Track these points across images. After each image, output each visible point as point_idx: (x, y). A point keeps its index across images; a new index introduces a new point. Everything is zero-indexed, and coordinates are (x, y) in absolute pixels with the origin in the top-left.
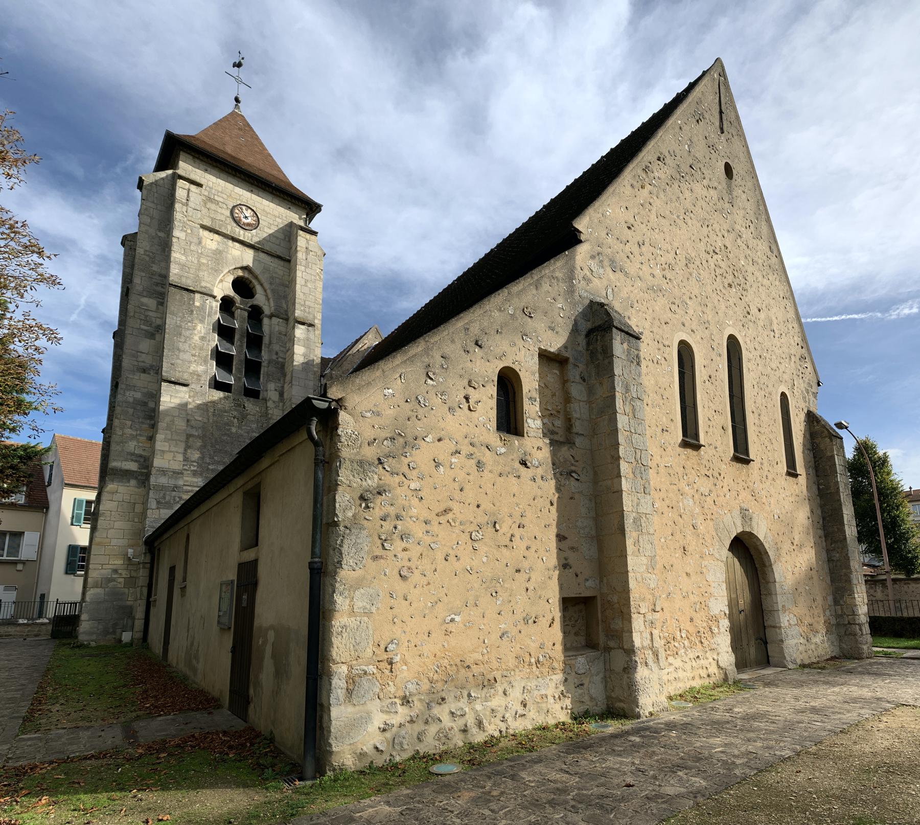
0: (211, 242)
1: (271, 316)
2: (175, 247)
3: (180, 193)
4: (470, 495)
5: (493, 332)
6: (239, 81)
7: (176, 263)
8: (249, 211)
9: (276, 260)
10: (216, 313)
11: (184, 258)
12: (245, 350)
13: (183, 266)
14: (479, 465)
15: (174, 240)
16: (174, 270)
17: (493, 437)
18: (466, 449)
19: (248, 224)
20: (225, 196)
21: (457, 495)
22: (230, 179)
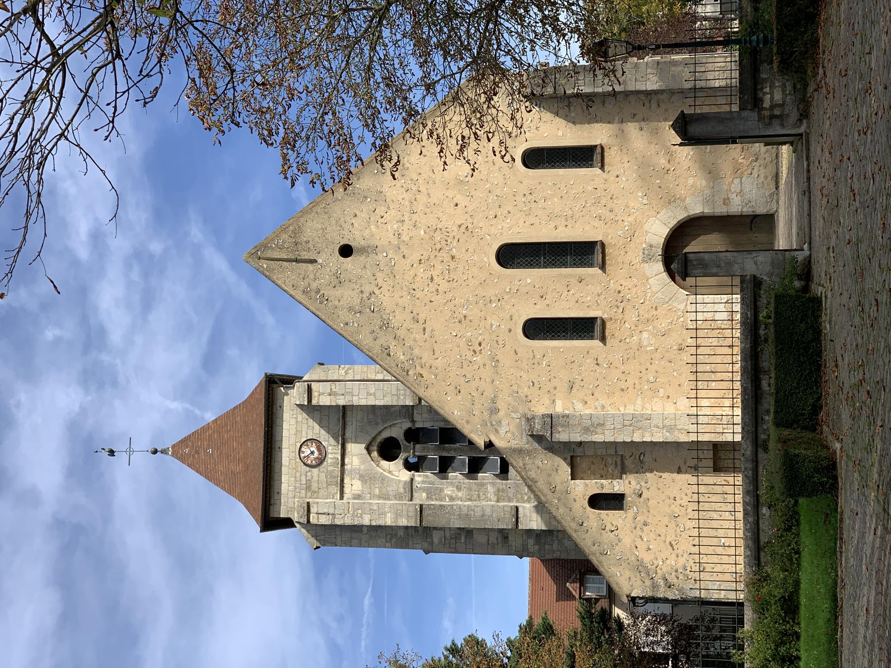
0: (353, 486)
1: (413, 421)
2: (381, 522)
3: (324, 520)
4: (662, 530)
5: (571, 513)
6: (130, 451)
7: (396, 521)
8: (303, 449)
9: (347, 419)
10: (427, 476)
11: (389, 515)
12: (458, 445)
13: (397, 515)
14: (645, 524)
15: (374, 523)
16: (403, 522)
17: (630, 513)
18: (639, 532)
19: (319, 450)
20: (298, 475)
21: (663, 538)
22: (276, 470)
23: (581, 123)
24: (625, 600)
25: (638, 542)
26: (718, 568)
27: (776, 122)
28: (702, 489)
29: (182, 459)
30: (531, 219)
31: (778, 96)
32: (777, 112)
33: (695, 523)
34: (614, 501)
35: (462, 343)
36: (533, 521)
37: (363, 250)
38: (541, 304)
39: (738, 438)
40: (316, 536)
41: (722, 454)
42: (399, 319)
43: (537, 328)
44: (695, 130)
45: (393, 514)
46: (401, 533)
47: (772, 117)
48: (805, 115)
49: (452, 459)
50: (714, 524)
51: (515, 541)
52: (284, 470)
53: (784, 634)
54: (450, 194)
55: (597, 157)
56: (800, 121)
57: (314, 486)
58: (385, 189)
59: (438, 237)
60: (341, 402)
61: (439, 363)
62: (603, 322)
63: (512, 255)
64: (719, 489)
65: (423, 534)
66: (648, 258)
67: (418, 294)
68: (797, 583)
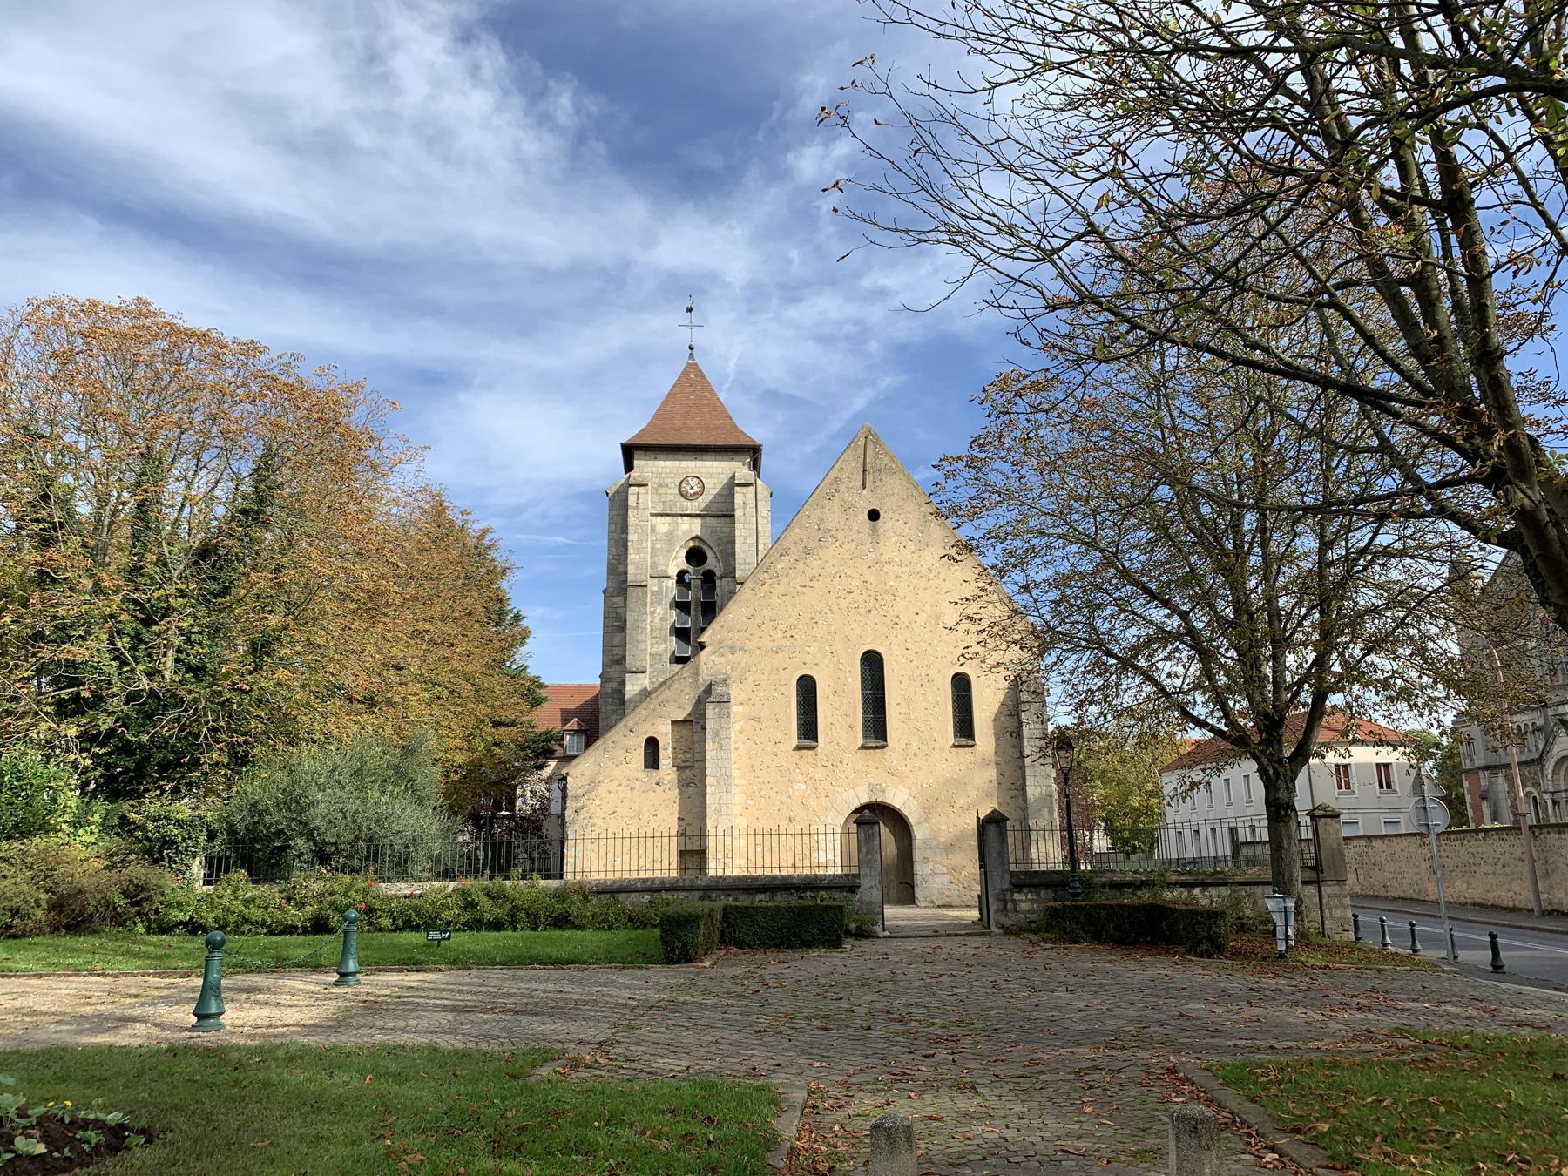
0: (663, 525)
2: (630, 551)
3: (632, 499)
6: (691, 326)
13: (638, 565)
16: (631, 570)
23: (995, 727)
24: (564, 771)
25: (616, 783)
26: (595, 856)
27: (1001, 904)
28: (666, 840)
29: (685, 372)
30: (906, 682)
31: (1024, 907)
32: (1009, 906)
33: (634, 834)
34: (652, 761)
35: (792, 621)
36: (633, 687)
37: (875, 531)
38: (829, 691)
39: (711, 873)
40: (617, 492)
41: (696, 858)
42: (814, 563)
43: (807, 688)
44: (992, 830)
45: (638, 562)
46: (621, 568)
47: (1005, 902)
48: (1008, 931)
49: (688, 613)
50: (634, 851)
51: (614, 671)
52: (676, 463)
53: (537, 916)
54: (927, 608)
55: (964, 741)
56: (1002, 927)
57: (662, 490)
58: (931, 550)
59: (889, 598)
60: (738, 513)
61: (774, 600)
62: (814, 748)
63: (873, 664)
64: (666, 854)
65: (619, 587)
66: (872, 789)
67: (836, 580)
68: (582, 928)
